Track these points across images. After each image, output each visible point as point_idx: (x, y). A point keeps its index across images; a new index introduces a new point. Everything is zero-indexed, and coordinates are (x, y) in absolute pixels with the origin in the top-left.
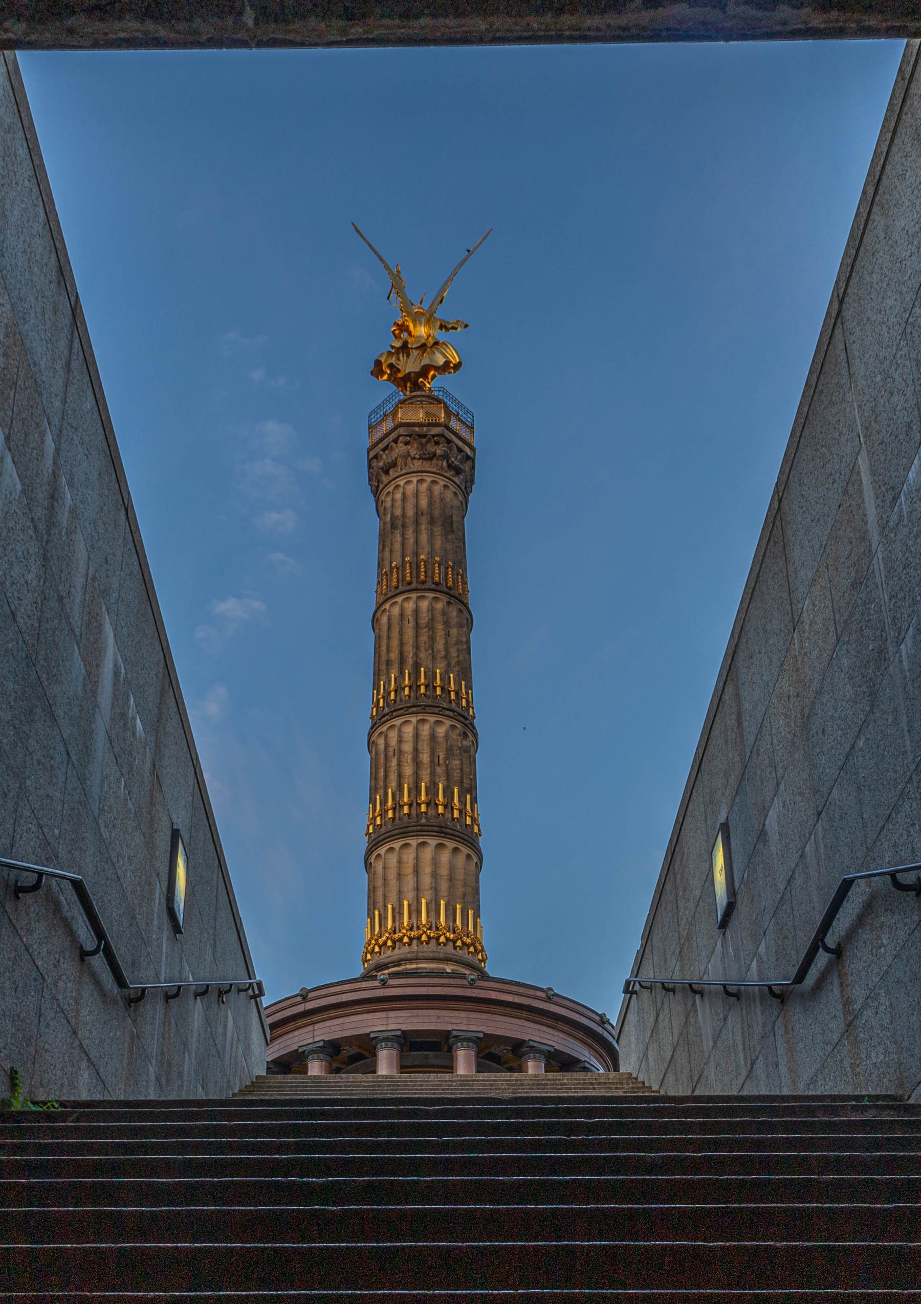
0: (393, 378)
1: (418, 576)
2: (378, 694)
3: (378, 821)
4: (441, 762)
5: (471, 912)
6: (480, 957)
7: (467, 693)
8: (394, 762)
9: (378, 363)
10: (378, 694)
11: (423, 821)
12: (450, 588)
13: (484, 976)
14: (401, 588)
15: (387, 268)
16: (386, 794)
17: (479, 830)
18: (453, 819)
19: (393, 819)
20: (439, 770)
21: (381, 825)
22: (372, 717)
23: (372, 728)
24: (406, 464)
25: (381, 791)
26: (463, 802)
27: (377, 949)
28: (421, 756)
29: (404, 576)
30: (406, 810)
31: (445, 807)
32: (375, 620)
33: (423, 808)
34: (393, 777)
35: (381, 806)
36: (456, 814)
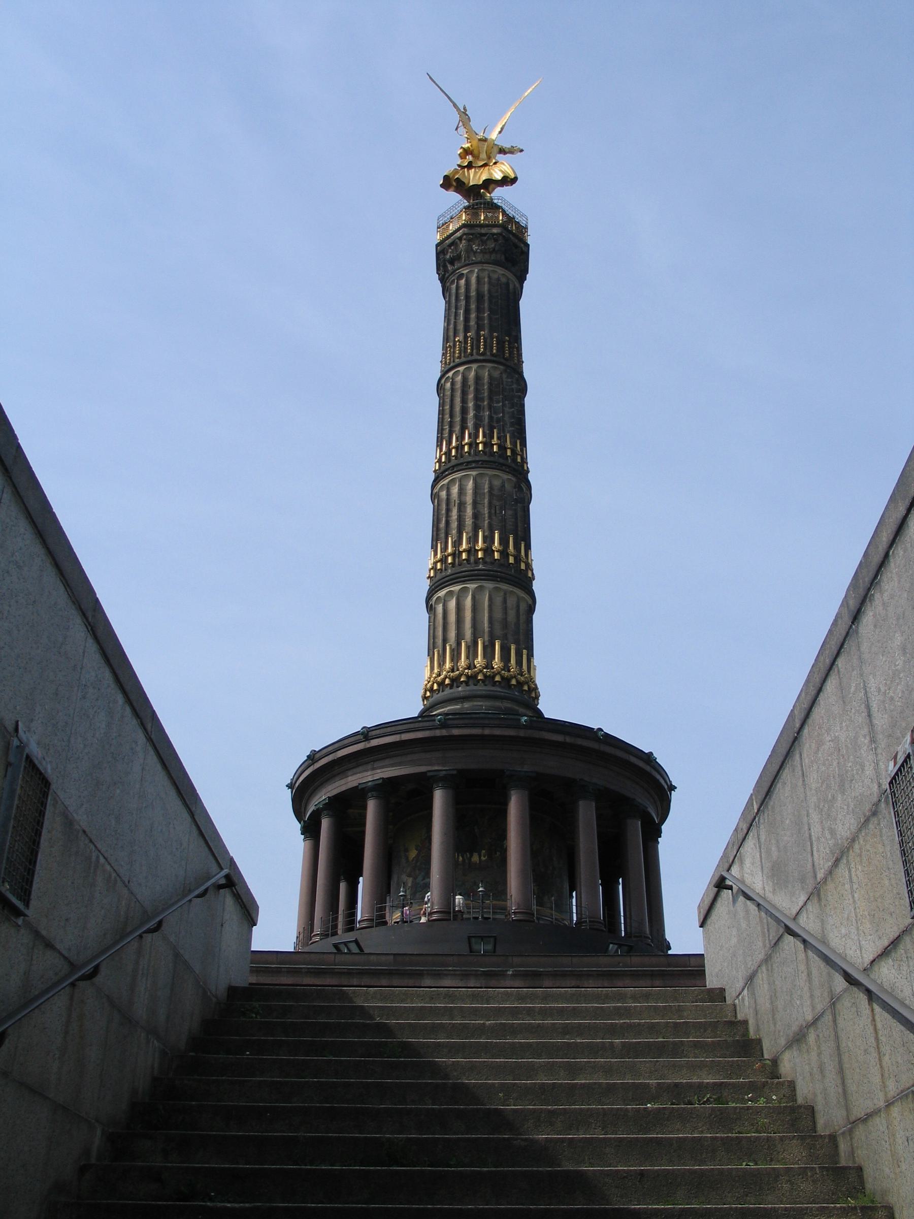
0: (457, 190)
1: (478, 348)
2: (441, 451)
3: (439, 566)
5: (525, 652)
6: (533, 695)
7: (522, 450)
9: (446, 178)
10: (441, 451)
12: (506, 359)
13: (539, 713)
14: (463, 359)
15: (455, 105)
16: (447, 542)
17: (533, 574)
22: (435, 471)
24: (468, 257)
26: (517, 547)
27: (435, 687)
29: (466, 349)
32: (440, 388)
35: (441, 552)
36: (511, 560)
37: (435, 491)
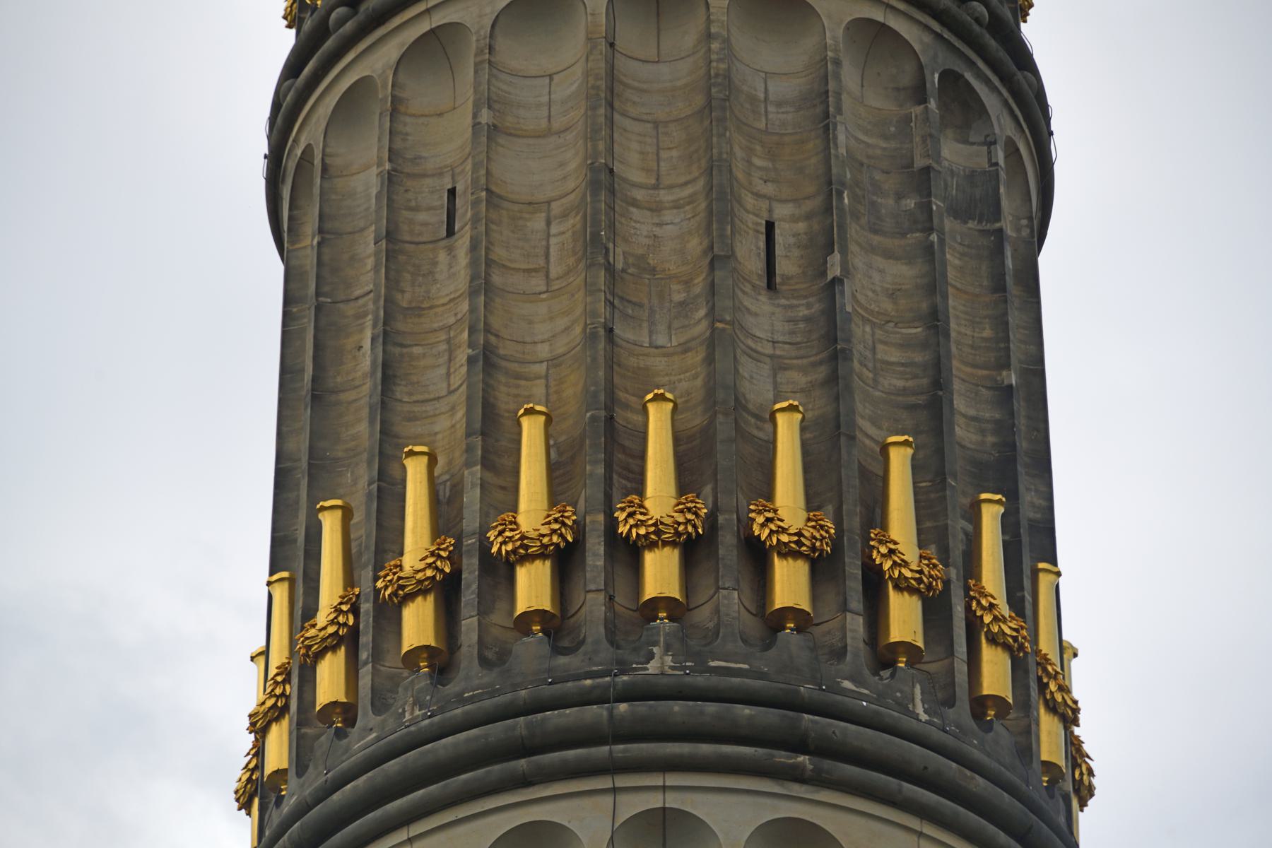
3: (330, 681)
4: (784, 266)
8: (451, 274)
11: (659, 665)
18: (884, 656)
19: (440, 660)
20: (766, 319)
21: (347, 711)
23: (292, 68)
25: (360, 480)
28: (640, 226)
30: (532, 587)
31: (823, 569)
33: (660, 573)
34: (443, 381)
36: (904, 619)
37: (310, 133)
